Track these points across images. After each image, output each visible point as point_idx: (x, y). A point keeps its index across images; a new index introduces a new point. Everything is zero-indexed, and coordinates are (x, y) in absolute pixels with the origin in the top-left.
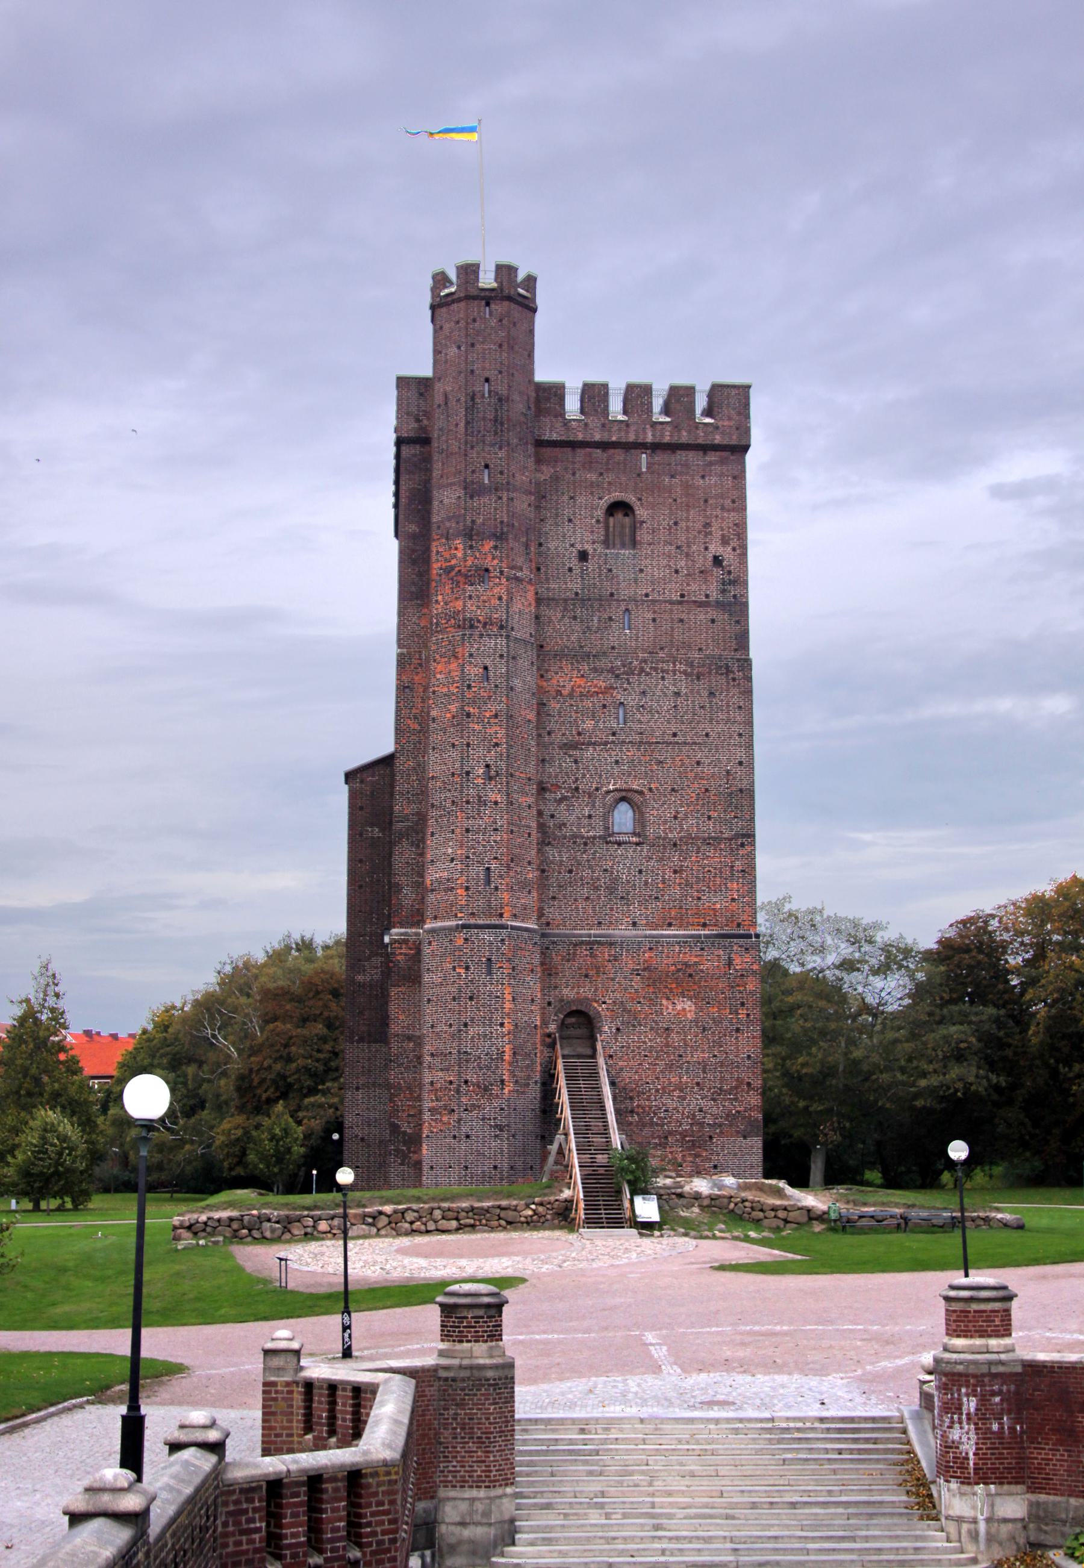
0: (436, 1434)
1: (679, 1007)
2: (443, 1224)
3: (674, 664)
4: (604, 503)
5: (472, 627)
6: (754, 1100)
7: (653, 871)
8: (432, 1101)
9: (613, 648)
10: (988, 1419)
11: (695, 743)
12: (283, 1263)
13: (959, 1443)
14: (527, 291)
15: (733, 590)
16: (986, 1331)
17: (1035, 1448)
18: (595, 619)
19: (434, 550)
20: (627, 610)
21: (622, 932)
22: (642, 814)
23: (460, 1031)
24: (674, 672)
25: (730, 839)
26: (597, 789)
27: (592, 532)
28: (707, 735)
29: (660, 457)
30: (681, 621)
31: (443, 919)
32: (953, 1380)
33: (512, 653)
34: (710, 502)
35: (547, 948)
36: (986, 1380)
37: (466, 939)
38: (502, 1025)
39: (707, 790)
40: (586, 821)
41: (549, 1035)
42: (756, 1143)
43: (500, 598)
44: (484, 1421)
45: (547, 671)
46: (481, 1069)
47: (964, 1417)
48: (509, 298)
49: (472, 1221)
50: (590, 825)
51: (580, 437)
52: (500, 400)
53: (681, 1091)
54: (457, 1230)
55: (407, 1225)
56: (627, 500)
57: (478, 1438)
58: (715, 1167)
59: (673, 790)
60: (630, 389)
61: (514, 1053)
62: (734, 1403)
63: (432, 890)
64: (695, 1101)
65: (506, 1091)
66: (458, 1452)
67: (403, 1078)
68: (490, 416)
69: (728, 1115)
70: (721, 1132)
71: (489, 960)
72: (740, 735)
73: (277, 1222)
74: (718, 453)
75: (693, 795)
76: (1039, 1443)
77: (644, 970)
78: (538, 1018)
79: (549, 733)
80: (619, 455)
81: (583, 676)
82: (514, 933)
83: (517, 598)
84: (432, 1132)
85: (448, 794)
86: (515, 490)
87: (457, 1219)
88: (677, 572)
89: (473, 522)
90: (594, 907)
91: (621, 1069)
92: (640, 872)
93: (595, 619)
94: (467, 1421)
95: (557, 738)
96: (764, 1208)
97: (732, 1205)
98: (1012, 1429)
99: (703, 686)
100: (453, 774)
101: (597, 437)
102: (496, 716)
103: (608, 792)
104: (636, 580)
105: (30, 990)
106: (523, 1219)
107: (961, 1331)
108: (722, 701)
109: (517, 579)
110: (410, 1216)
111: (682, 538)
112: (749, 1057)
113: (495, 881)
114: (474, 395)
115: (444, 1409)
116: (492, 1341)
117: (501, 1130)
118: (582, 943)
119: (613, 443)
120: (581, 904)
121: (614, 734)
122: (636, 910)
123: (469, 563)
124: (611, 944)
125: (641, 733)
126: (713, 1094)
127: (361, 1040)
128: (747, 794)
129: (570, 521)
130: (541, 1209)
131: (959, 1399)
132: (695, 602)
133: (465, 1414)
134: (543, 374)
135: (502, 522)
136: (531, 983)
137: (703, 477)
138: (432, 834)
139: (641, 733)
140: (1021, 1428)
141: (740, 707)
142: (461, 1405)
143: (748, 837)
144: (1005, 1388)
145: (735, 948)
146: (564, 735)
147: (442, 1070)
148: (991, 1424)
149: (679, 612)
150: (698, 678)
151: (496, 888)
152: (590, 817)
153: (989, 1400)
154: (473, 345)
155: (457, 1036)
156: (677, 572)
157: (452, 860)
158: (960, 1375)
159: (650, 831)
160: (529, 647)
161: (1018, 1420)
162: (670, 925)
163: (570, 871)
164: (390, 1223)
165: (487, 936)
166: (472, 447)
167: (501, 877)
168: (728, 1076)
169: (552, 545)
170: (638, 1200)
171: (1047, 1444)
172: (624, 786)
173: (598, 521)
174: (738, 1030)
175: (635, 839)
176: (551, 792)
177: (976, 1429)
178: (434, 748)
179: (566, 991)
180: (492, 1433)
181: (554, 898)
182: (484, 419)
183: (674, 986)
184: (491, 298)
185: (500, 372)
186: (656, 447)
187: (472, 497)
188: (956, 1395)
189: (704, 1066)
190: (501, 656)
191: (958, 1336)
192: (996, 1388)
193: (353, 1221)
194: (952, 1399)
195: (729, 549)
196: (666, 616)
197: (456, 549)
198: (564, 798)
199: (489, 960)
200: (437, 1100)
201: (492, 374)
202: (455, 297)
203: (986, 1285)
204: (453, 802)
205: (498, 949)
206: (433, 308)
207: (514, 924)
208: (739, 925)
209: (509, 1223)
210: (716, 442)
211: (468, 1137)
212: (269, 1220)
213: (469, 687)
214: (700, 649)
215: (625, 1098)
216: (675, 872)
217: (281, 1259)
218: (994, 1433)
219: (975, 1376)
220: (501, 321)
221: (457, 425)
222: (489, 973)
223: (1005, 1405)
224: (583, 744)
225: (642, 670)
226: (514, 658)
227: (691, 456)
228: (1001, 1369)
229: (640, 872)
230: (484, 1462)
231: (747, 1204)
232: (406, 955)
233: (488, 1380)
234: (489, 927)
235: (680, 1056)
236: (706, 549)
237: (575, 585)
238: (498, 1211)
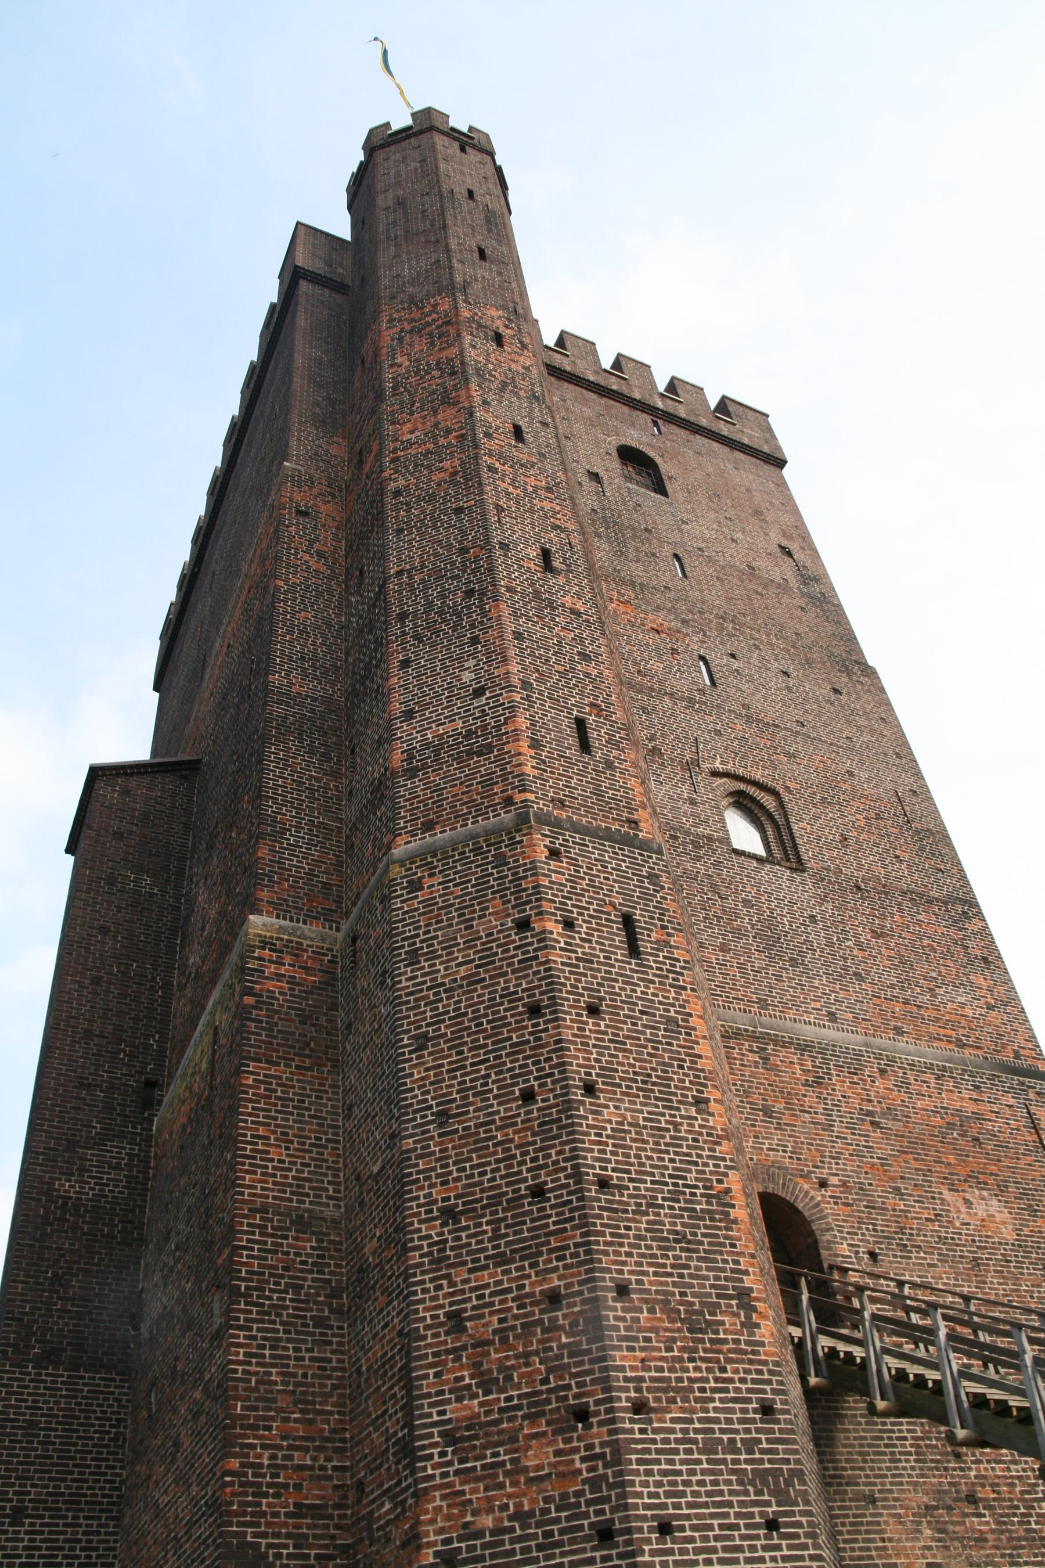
8: (461, 1393)
15: (816, 589)
37: (554, 854)
67: (280, 1361)
71: (628, 921)
84: (471, 1533)
100: (464, 551)
127: (50, 1357)
138: (405, 664)
147: (501, 1260)
172: (741, 772)
199: (628, 921)
200: (487, 1384)
222: (634, 950)
232: (292, 981)
234: (609, 836)
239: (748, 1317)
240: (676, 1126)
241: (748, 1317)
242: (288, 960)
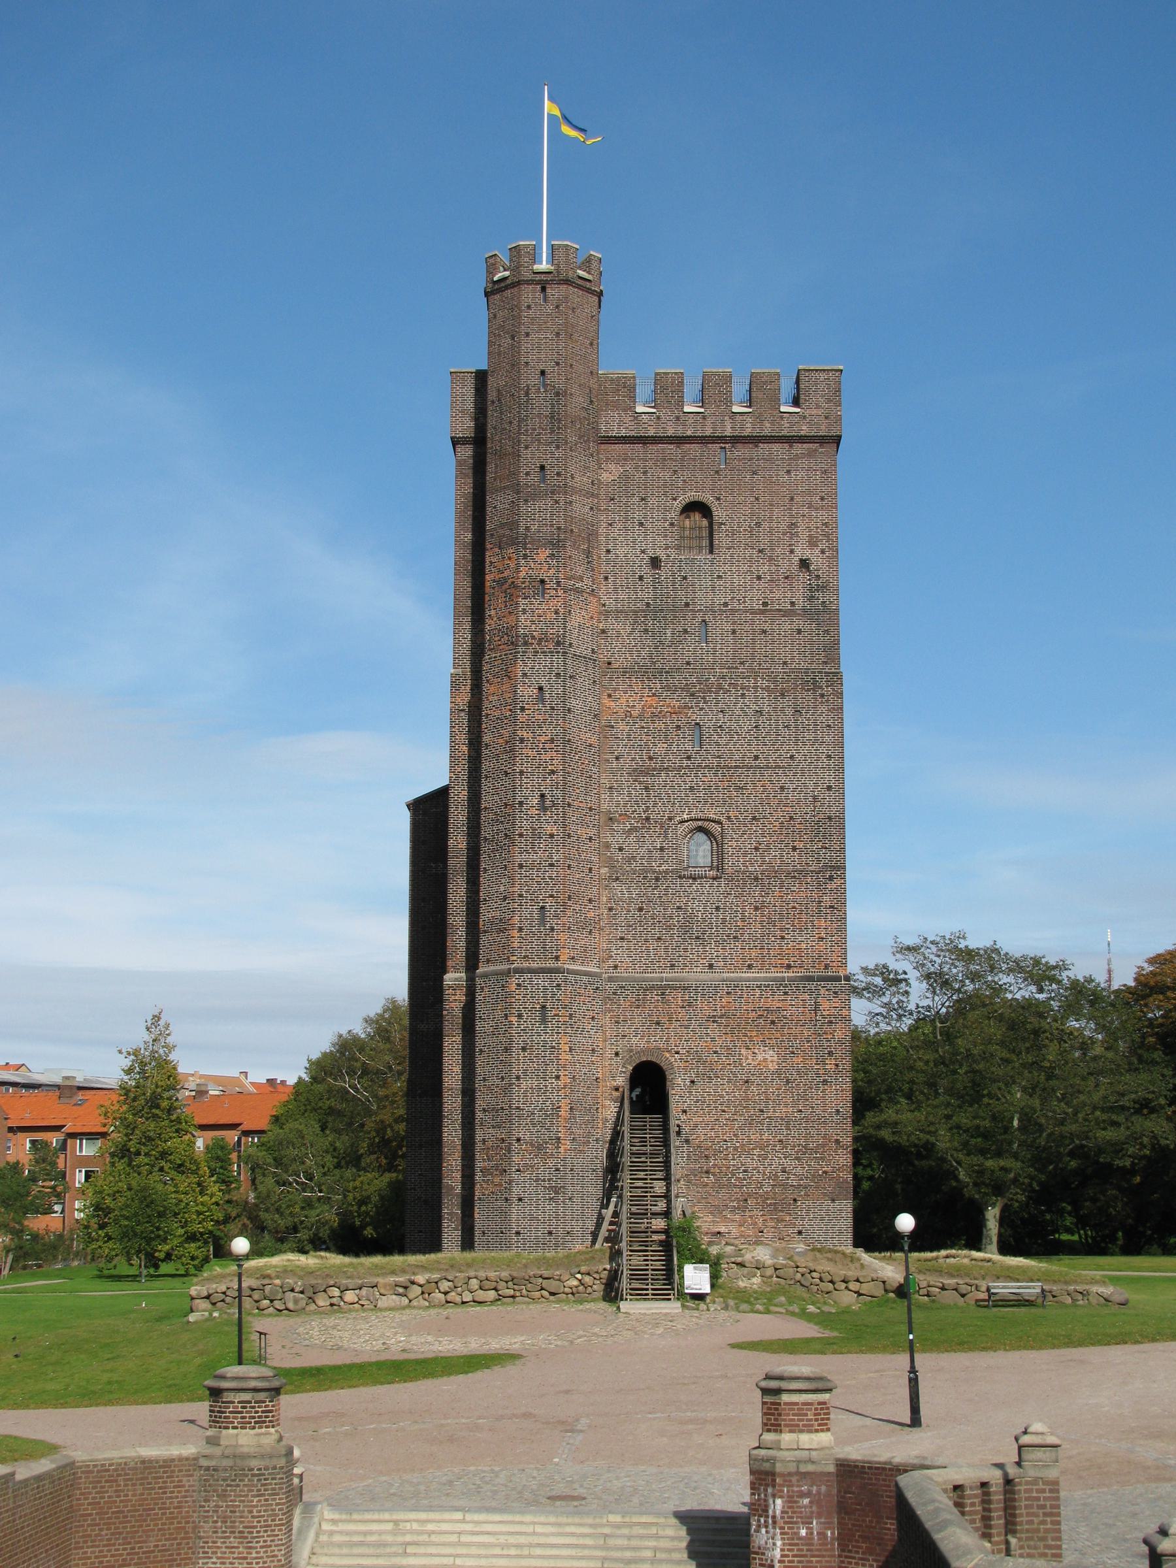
0: (194, 1528)
1: (760, 1057)
2: (481, 1295)
3: (755, 679)
4: (678, 505)
5: (526, 643)
6: (844, 1159)
7: (731, 909)
9: (688, 663)
10: (796, 1523)
11: (779, 767)
12: (263, 1336)
13: (765, 1549)
14: (589, 273)
16: (798, 1425)
17: (846, 1557)
18: (669, 632)
19: (487, 560)
20: (704, 621)
21: (697, 975)
22: (720, 845)
23: (511, 1085)
24: (755, 687)
26: (670, 819)
27: (666, 536)
28: (792, 757)
29: (742, 451)
30: (764, 632)
31: (494, 962)
32: (761, 1479)
33: (570, 672)
34: (797, 499)
35: (614, 993)
36: (794, 1479)
37: (519, 985)
38: (558, 1077)
39: (791, 818)
40: (657, 854)
41: (617, 1089)
42: (845, 1209)
43: (556, 613)
44: (246, 1514)
45: (615, 690)
46: (534, 1125)
47: (770, 1521)
48: (567, 282)
49: (511, 1292)
50: (662, 858)
51: (651, 432)
52: (557, 394)
54: (493, 1302)
55: (442, 1296)
56: (705, 501)
57: (240, 1532)
58: (800, 1233)
59: (754, 818)
60: (706, 377)
61: (571, 1108)
62: (584, 1498)
63: (485, 932)
64: (777, 1162)
65: (562, 1150)
66: (218, 1547)
68: (547, 412)
69: (813, 1176)
71: (544, 1007)
72: (829, 756)
73: (302, 1292)
74: (805, 445)
76: (850, 1551)
77: (721, 1017)
79: (617, 758)
80: (694, 449)
81: (654, 695)
82: (571, 977)
83: (576, 612)
85: (501, 827)
86: (574, 491)
87: (495, 1289)
88: (759, 578)
89: (527, 529)
90: (666, 948)
91: (696, 1126)
92: (717, 908)
93: (669, 632)
94: (228, 1513)
95: (626, 762)
96: (836, 1279)
97: (798, 1276)
98: (822, 1535)
99: (787, 701)
102: (552, 741)
104: (713, 588)
105: (139, 1037)
106: (567, 1290)
107: (772, 1425)
108: (808, 720)
109: (579, 591)
110: (445, 1286)
111: (765, 542)
112: (838, 1111)
113: (551, 921)
114: (528, 389)
115: (205, 1501)
116: (260, 1427)
117: (556, 1193)
118: (653, 987)
120: (653, 944)
121: (689, 758)
122: (712, 950)
123: (522, 574)
124: (685, 988)
125: (719, 757)
126: (797, 1152)
128: (836, 822)
129: (641, 524)
130: (587, 1279)
131: (765, 1501)
132: (780, 610)
133: (227, 1506)
134: (610, 365)
135: (559, 528)
137: (788, 472)
139: (719, 757)
140: (833, 1533)
141: (829, 726)
142: (223, 1496)
143: (838, 869)
144: (814, 1489)
145: (822, 991)
146: (633, 759)
148: (799, 1528)
149: (761, 622)
150: (783, 695)
151: (552, 929)
152: (662, 849)
153: (798, 1502)
154: (527, 335)
155: (507, 1089)
156: (759, 578)
157: (505, 898)
158: (767, 1473)
159: (729, 863)
160: (591, 665)
161: (828, 1525)
162: (750, 967)
163: (641, 909)
164: (423, 1293)
165: (541, 981)
166: (527, 447)
167: (556, 916)
168: (813, 1132)
169: (621, 552)
170: (689, 1269)
171: (857, 1552)
173: (672, 524)
174: (825, 1081)
175: (713, 873)
176: (619, 822)
177: (781, 1534)
178: (486, 777)
179: (634, 1040)
180: (256, 1527)
181: (622, 938)
182: (540, 414)
183: (754, 1034)
184: (547, 282)
185: (558, 364)
186: (736, 440)
187: (526, 501)
188: (763, 1496)
189: (787, 1122)
190: (558, 675)
191: (769, 1431)
192: (804, 1488)
193: (382, 1291)
194: (759, 1500)
195: (817, 551)
196: (747, 627)
197: (510, 558)
198: (635, 829)
199: (544, 1007)
200: (489, 1159)
201: (549, 367)
202: (508, 282)
203: (799, 1375)
204: (506, 834)
205: (554, 995)
206: (487, 294)
207: (571, 967)
208: (826, 967)
209: (552, 1294)
210: (803, 433)
211: (520, 1200)
212: (292, 1290)
213: (523, 709)
214: (785, 663)
215: (701, 1157)
216: (756, 909)
217: (261, 1333)
218: (800, 1538)
219: (782, 1475)
220: (557, 307)
221: (511, 423)
222: (544, 1020)
223: (814, 1508)
224: (654, 769)
225: (720, 687)
227: (776, 447)
228: (810, 1468)
229: (717, 908)
230: (246, 1558)
231: (814, 1274)
233: (253, 1469)
235: (762, 1111)
236: (792, 552)
237: (646, 594)
238: (540, 1280)
239: (558, 1145)
240: (546, 1087)
241: (558, 1145)
242: (458, 992)
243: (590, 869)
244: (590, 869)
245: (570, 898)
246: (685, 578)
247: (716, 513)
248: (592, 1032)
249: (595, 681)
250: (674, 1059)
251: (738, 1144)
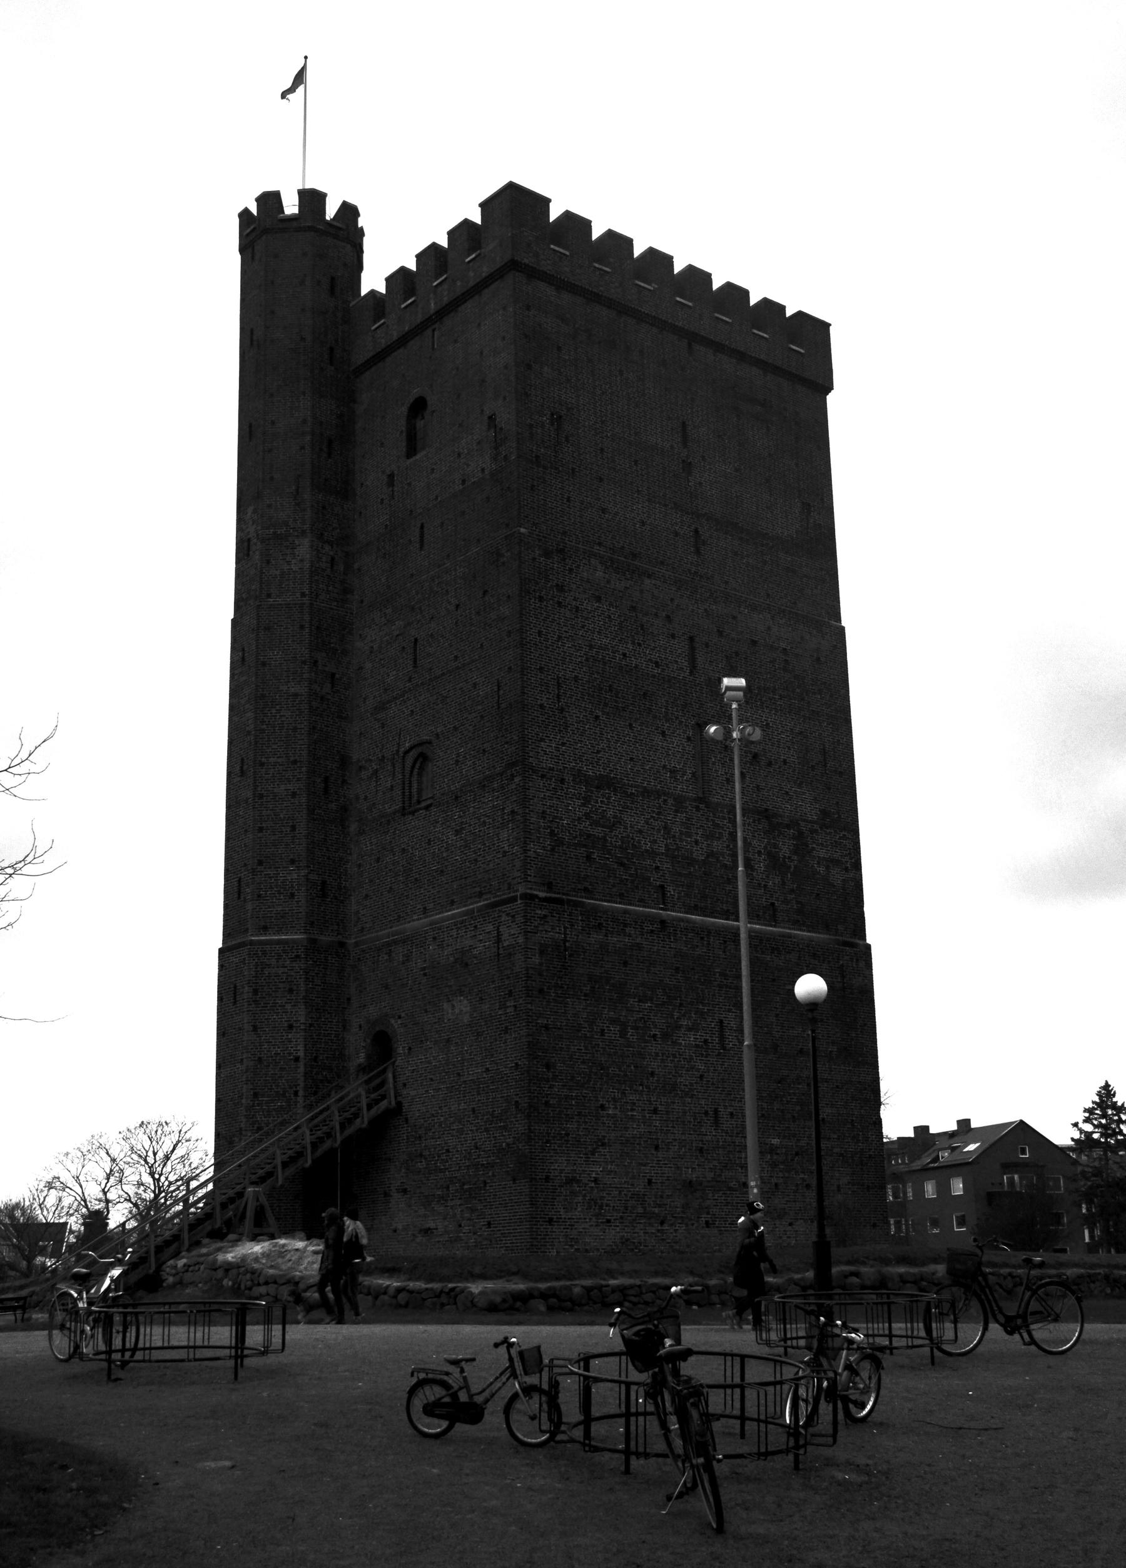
4: (404, 410)
21: (416, 923)
25: (501, 774)
26: (398, 751)
53: (460, 1122)
61: (256, 1095)
70: (494, 1175)
71: (235, 987)
75: (471, 728)
78: (301, 1048)
88: (459, 455)
101: (395, 336)
103: (407, 752)
119: (407, 333)
121: (410, 680)
136: (288, 1007)
162: (452, 902)
173: (402, 432)
198: (376, 772)
199: (235, 987)
210: (484, 275)
226: (267, 629)
235: (459, 1074)
243: (293, 828)
244: (293, 828)
245: (260, 863)
246: (409, 484)
247: (429, 403)
248: (288, 1007)
249: (302, 627)
250: (395, 1023)
251: (442, 1119)
